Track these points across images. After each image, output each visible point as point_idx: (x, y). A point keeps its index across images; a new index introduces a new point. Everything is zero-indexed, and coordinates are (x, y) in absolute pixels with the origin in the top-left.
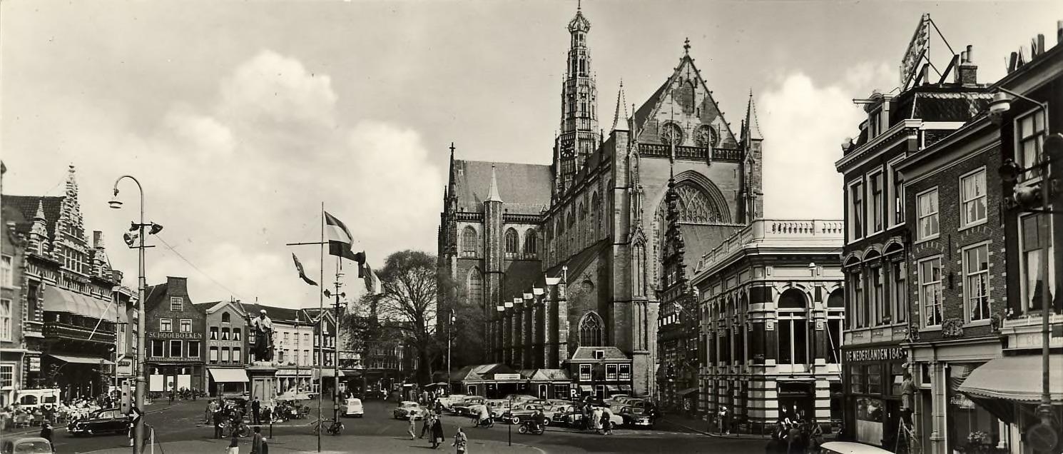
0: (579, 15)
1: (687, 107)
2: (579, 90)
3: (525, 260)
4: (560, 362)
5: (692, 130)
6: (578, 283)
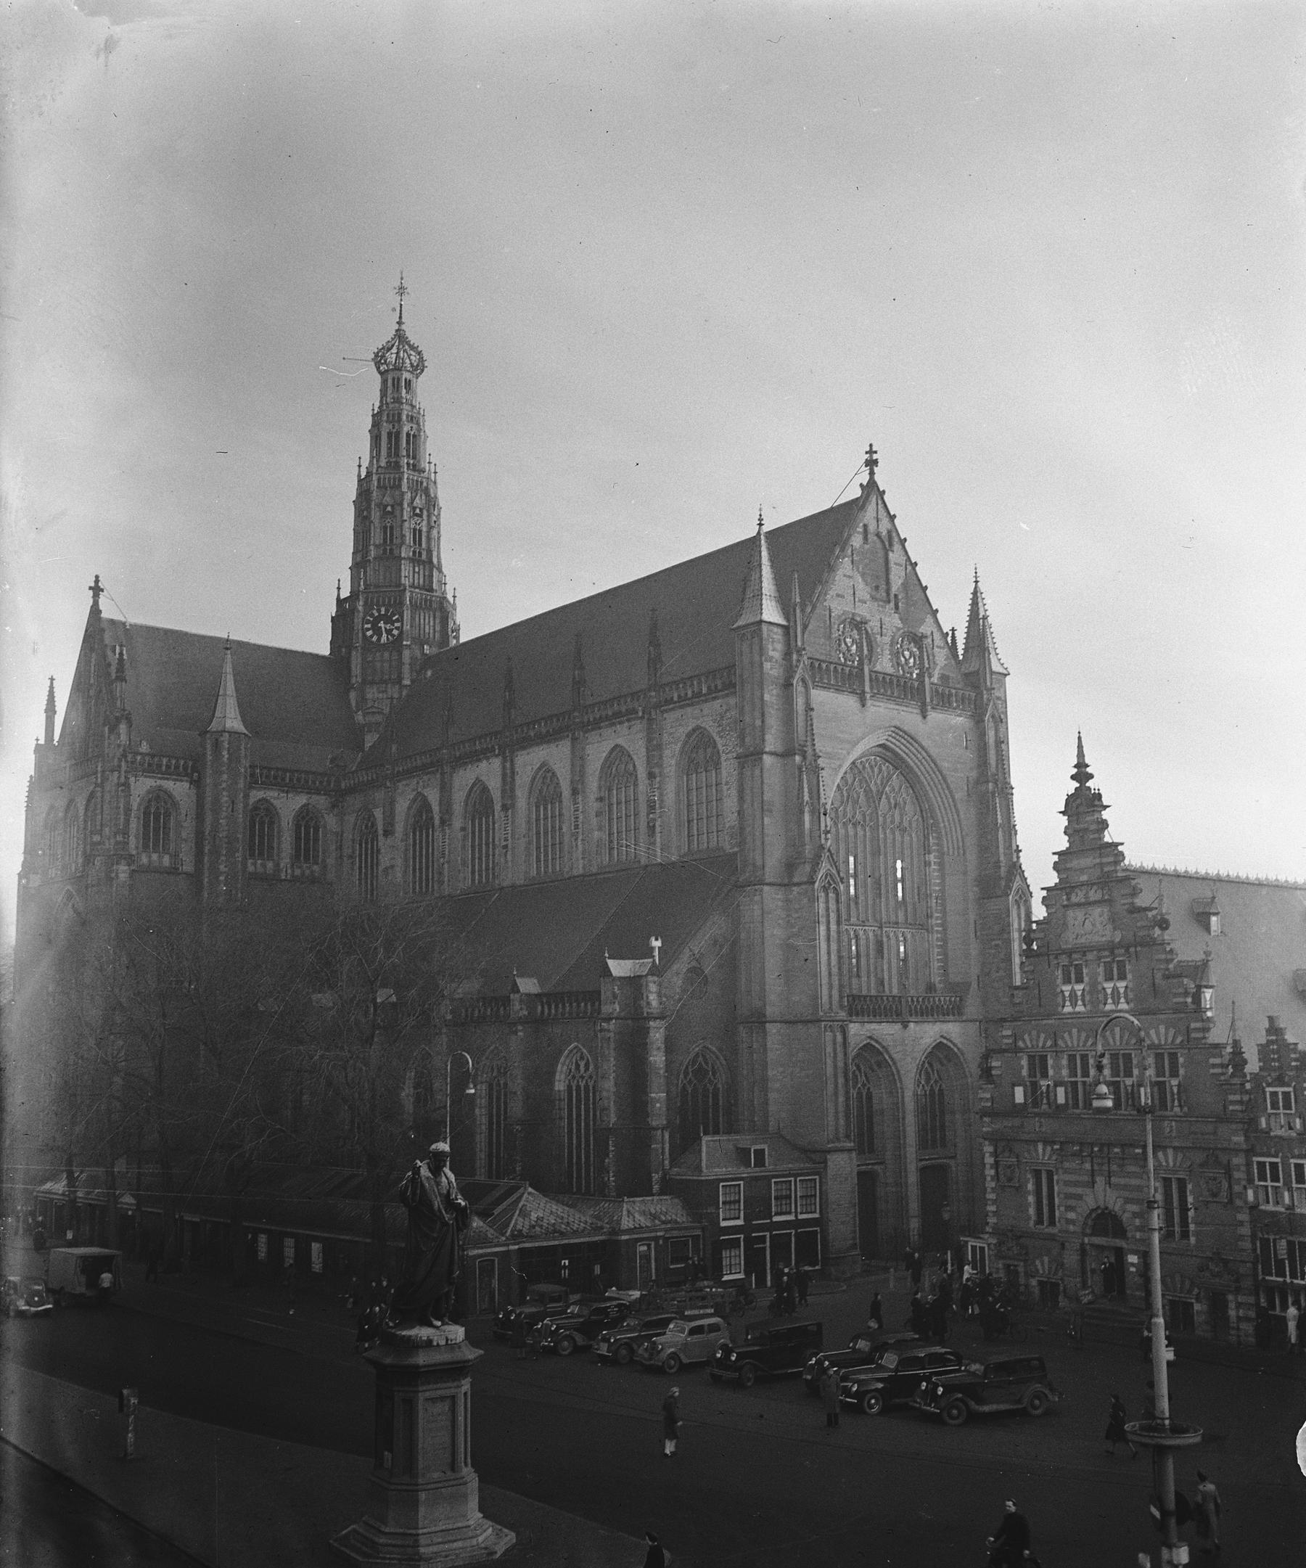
0: (400, 336)
1: (877, 588)
2: (408, 496)
3: (295, 879)
4: (655, 1177)
5: (887, 639)
6: (678, 974)
